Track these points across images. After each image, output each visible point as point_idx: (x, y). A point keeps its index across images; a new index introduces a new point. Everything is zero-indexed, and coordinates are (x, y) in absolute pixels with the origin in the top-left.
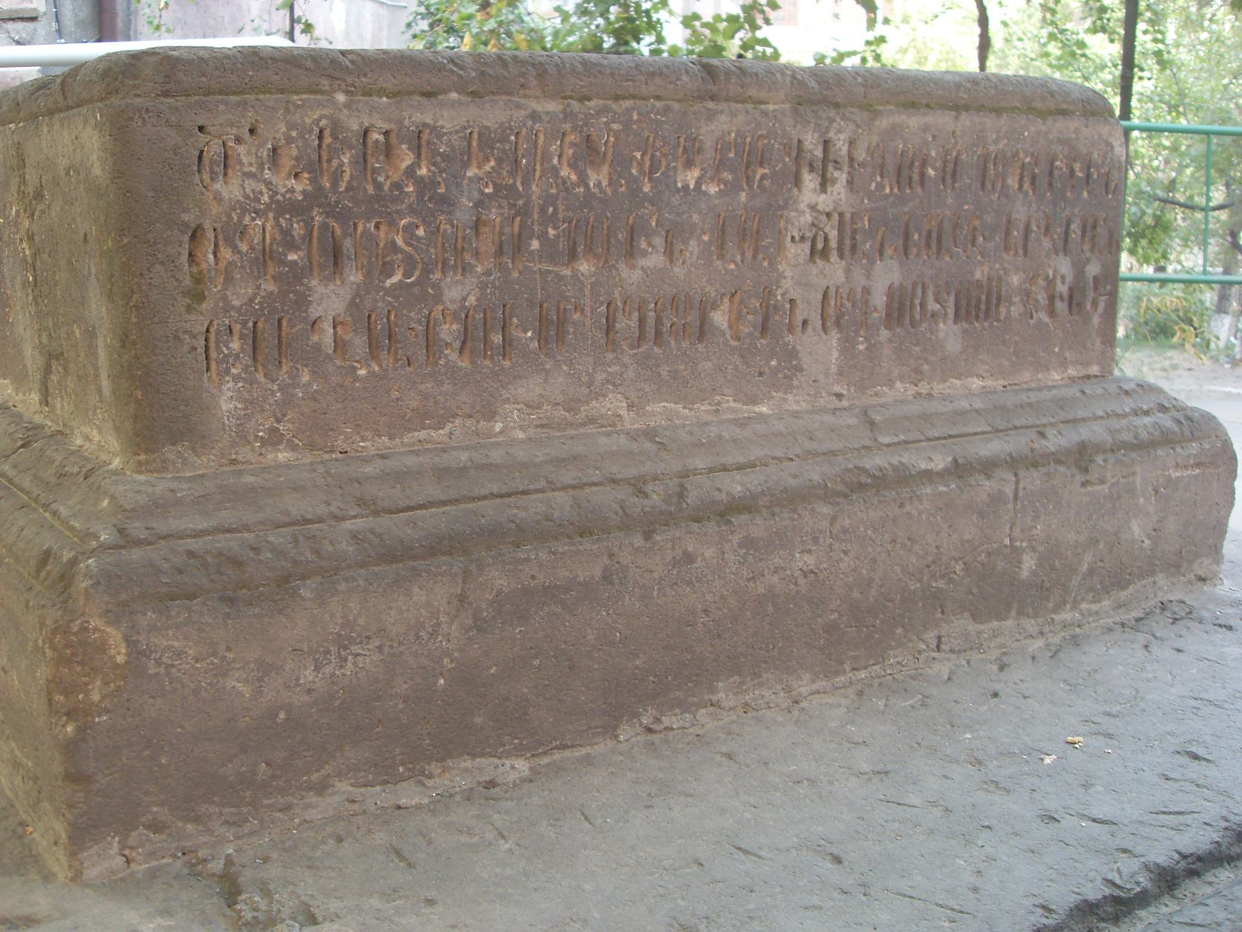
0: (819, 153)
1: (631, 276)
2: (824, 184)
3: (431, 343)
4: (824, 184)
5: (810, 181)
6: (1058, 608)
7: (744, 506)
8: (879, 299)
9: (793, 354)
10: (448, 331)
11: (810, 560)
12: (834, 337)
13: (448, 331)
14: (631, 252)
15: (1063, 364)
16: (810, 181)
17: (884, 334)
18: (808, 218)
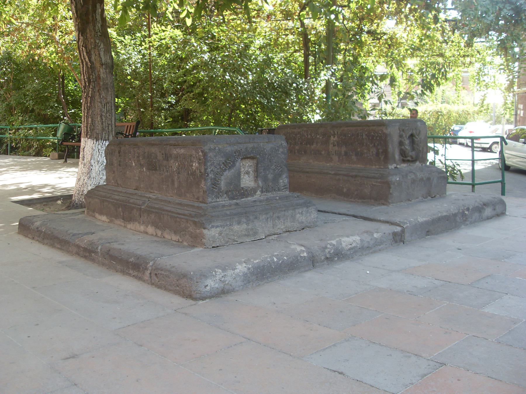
0: (333, 133)
1: (313, 147)
2: (334, 137)
3: (295, 153)
4: (334, 137)
5: (332, 137)
6: (351, 198)
7: (307, 172)
8: (343, 153)
9: (332, 158)
10: (296, 151)
11: (314, 180)
12: (337, 157)
13: (296, 151)
14: (312, 145)
15: (375, 165)
16: (332, 137)
17: (344, 157)
18: (332, 141)
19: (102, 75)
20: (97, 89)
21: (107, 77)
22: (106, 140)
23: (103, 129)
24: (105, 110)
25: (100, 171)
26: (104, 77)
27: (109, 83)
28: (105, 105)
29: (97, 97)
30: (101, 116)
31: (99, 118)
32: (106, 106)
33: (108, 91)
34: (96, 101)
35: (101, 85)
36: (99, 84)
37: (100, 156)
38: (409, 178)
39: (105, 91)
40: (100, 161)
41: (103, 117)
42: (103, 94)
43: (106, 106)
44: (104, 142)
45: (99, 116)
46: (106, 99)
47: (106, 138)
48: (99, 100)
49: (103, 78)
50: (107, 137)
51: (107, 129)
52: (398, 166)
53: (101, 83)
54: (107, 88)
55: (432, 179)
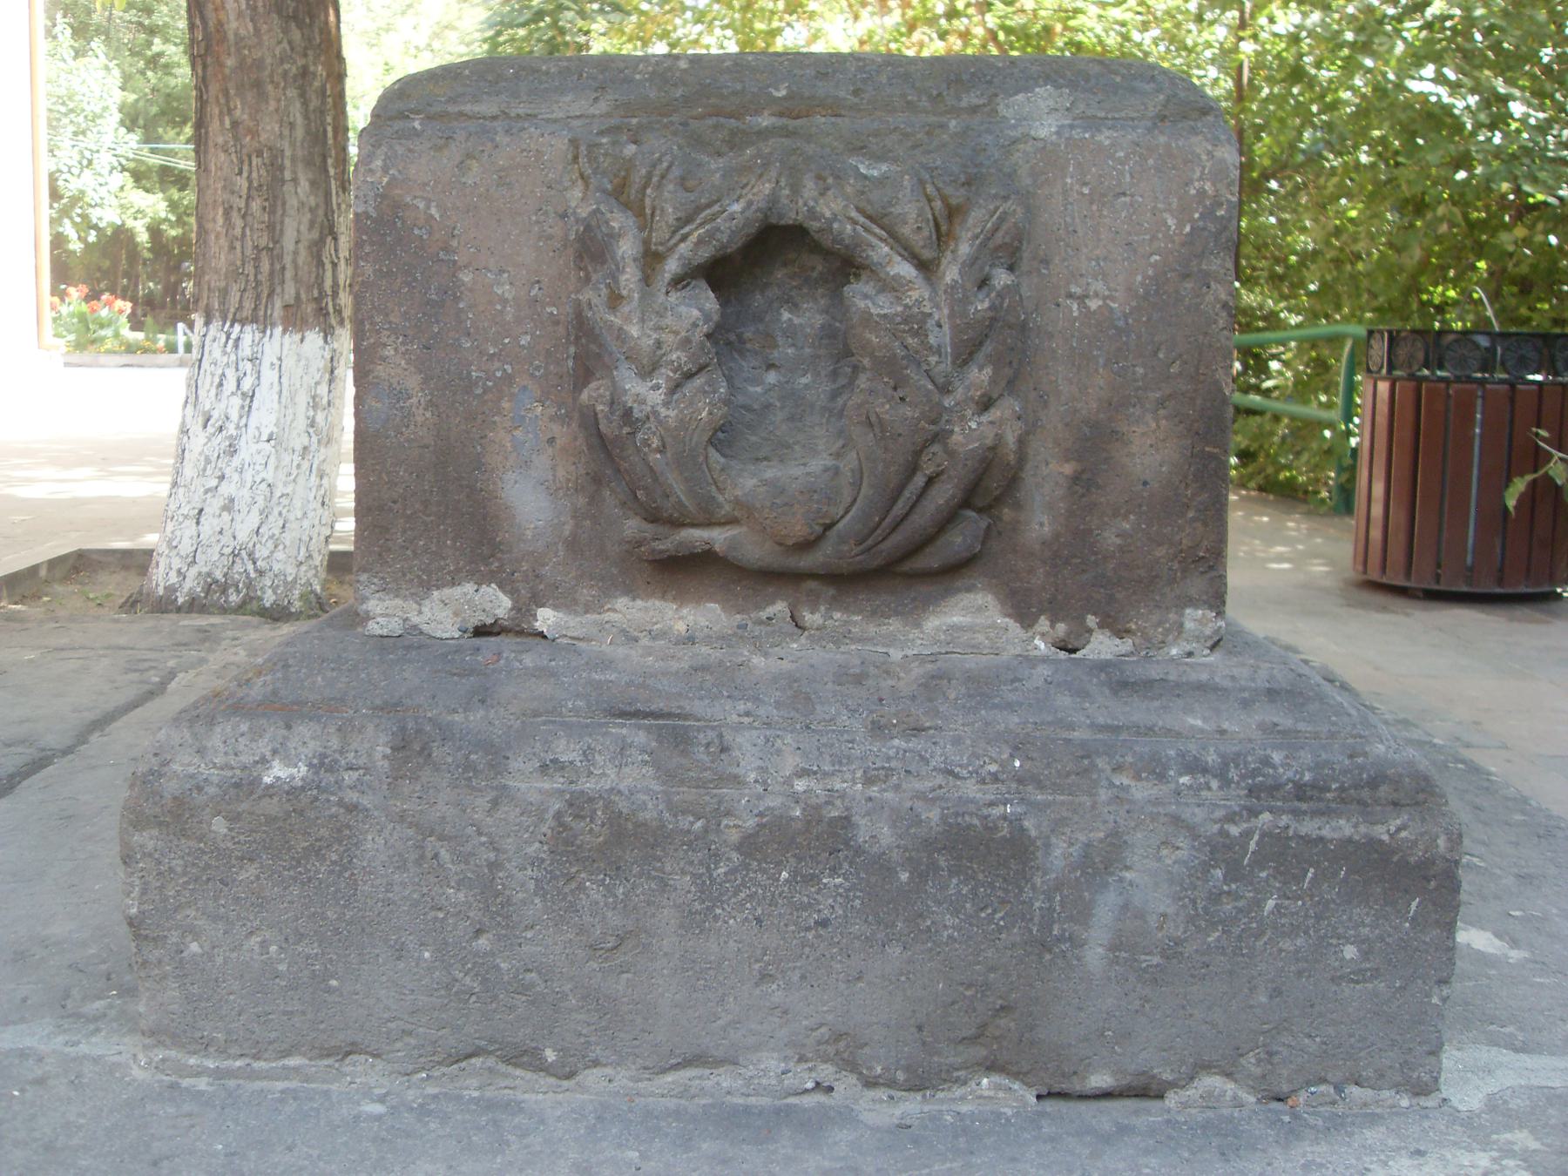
19: (232, 25)
20: (214, 88)
21: (257, 30)
22: (243, 322)
23: (235, 274)
24: (245, 185)
25: (208, 461)
26: (242, 32)
27: (269, 61)
28: (242, 162)
29: (214, 126)
30: (227, 213)
31: (220, 221)
32: (246, 168)
33: (262, 96)
34: (211, 144)
35: (227, 71)
36: (221, 65)
37: (213, 391)
38: (526, 782)
39: (250, 96)
40: (215, 414)
41: (235, 214)
42: (238, 112)
43: (246, 168)
44: (237, 327)
45: (221, 211)
46: (255, 134)
47: (247, 312)
48: (220, 140)
49: (239, 39)
50: (248, 305)
51: (250, 269)
52: (546, 618)
53: (230, 62)
54: (258, 85)
55: (1059, 855)
